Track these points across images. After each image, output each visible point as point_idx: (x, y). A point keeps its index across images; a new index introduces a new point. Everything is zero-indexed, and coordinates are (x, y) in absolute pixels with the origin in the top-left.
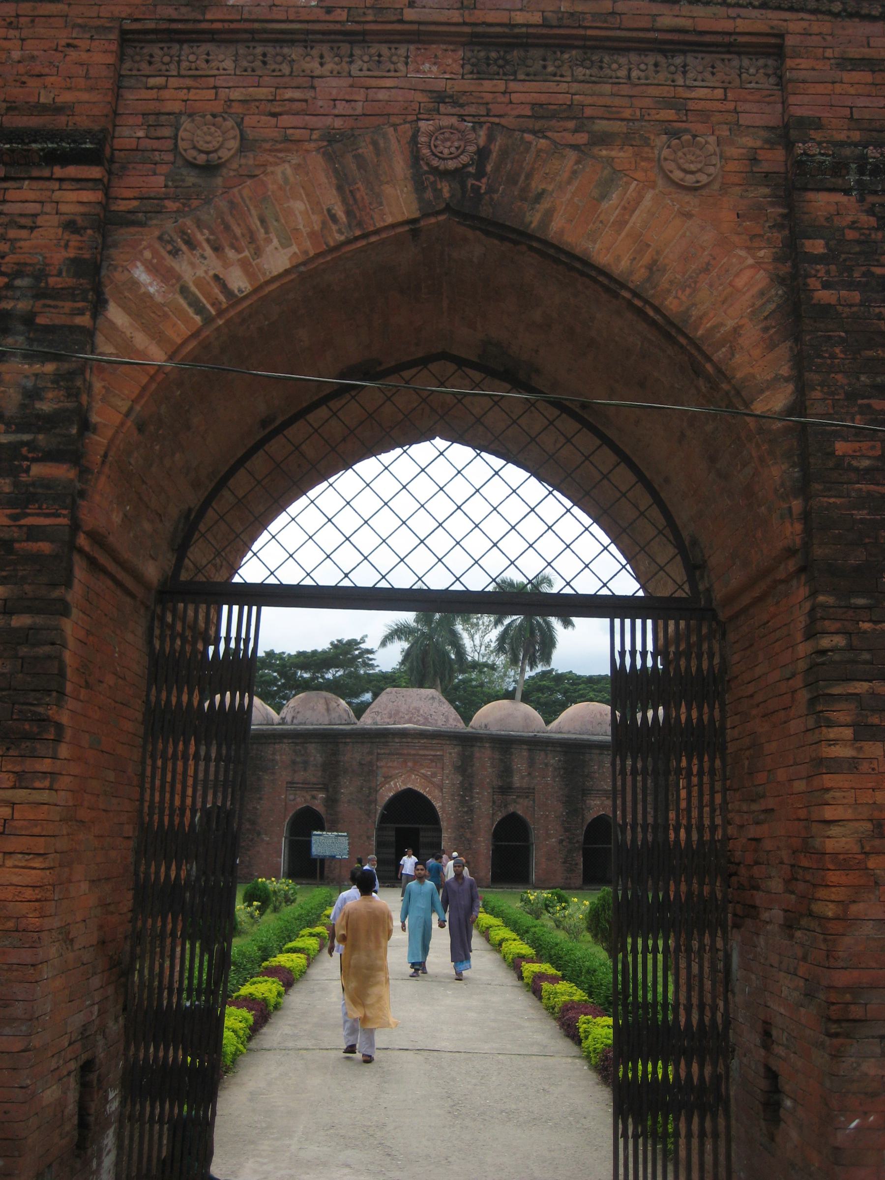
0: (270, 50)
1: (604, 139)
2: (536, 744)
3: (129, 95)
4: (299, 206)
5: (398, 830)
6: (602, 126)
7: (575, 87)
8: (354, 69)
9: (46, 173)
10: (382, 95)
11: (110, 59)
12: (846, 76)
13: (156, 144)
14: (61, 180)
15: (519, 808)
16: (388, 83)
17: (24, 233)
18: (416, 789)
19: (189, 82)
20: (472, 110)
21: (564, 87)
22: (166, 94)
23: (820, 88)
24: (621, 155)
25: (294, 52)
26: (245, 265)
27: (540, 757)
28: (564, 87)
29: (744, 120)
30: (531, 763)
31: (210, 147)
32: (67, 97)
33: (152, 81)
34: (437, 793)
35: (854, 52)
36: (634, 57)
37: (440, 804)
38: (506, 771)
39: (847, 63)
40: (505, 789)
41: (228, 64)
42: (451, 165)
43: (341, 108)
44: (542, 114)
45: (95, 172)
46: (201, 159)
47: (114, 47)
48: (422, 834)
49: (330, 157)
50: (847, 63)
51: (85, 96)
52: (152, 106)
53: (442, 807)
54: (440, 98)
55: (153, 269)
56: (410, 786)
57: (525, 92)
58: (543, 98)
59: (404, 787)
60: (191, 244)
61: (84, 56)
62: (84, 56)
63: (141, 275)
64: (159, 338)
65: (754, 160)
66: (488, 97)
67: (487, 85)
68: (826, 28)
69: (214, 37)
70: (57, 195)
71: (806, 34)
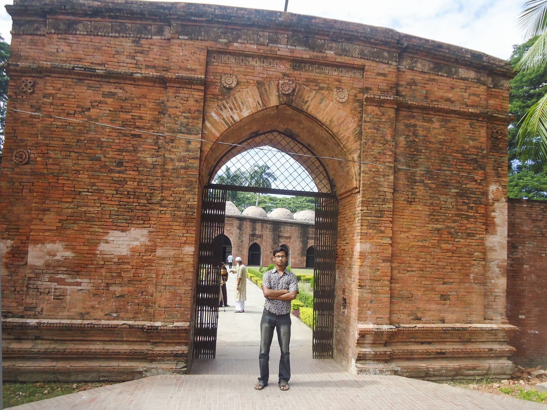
0: (244, 58)
1: (322, 88)
2: (264, 222)
4: (251, 100)
6: (321, 85)
7: (316, 74)
8: (264, 65)
9: (190, 87)
10: (271, 73)
11: (205, 58)
12: (379, 77)
13: (216, 81)
14: (194, 89)
15: (257, 241)
16: (272, 70)
17: (185, 102)
19: (224, 65)
20: (292, 78)
21: (313, 74)
22: (219, 67)
23: (372, 80)
24: (325, 92)
25: (250, 59)
27: (265, 225)
28: (313, 74)
29: (354, 86)
30: (262, 227)
31: (229, 83)
32: (194, 67)
33: (215, 64)
35: (381, 72)
36: (330, 68)
38: (254, 229)
39: (379, 74)
40: (253, 235)
41: (234, 61)
42: (287, 93)
43: (261, 75)
44: (308, 80)
45: (203, 88)
46: (228, 86)
47: (206, 54)
49: (258, 88)
50: (379, 74)
54: (285, 75)
55: (217, 113)
57: (305, 75)
58: (308, 77)
60: (225, 108)
61: (198, 56)
62: (198, 56)
63: (213, 114)
64: (218, 130)
65: (356, 96)
66: (296, 75)
67: (296, 72)
69: (229, 53)
71: (370, 66)
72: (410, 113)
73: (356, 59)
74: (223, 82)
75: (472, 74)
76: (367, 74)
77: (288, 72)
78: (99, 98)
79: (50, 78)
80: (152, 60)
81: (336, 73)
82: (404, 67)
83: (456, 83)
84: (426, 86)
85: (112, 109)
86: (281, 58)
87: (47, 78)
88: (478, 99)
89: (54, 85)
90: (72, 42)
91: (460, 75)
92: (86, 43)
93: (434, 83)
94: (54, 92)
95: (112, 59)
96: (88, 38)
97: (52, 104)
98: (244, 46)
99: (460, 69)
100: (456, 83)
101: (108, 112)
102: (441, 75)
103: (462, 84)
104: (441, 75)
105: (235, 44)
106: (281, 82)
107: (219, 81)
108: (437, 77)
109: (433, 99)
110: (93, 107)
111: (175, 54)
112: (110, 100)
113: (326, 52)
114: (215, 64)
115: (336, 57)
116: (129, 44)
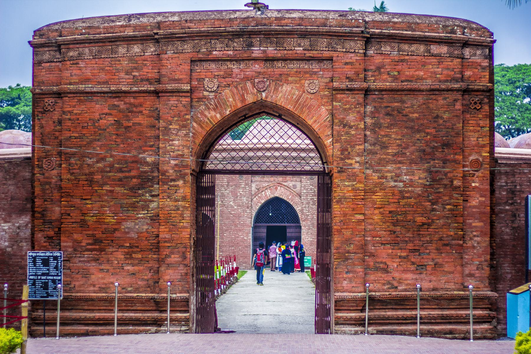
0: (223, 62)
3: (193, 74)
5: (268, 228)
7: (288, 70)
8: (241, 66)
10: (247, 73)
12: (346, 67)
16: (248, 70)
17: (175, 108)
18: (281, 197)
19: (206, 71)
20: (266, 76)
21: (286, 70)
23: (340, 70)
25: (228, 63)
26: (220, 113)
28: (286, 70)
32: (181, 77)
34: (297, 199)
35: (348, 61)
37: (300, 208)
41: (214, 66)
43: (238, 76)
45: (189, 94)
46: (210, 90)
48: (288, 230)
50: (346, 64)
51: (185, 77)
52: (199, 77)
53: (302, 211)
54: (259, 73)
56: (277, 195)
59: (272, 196)
61: (184, 67)
62: (184, 67)
66: (270, 73)
68: (342, 54)
70: (181, 99)
71: (338, 56)
72: (380, 96)
73: (324, 52)
74: (206, 87)
75: (444, 49)
76: (336, 65)
77: (262, 71)
78: (106, 111)
79: (67, 98)
80: (146, 74)
81: (306, 67)
82: (372, 52)
83: (427, 61)
84: (396, 67)
85: (116, 119)
86: (255, 60)
87: (65, 98)
88: (453, 73)
89: (70, 103)
90: (81, 66)
91: (432, 51)
92: (93, 65)
93: (405, 64)
94: (70, 109)
95: (114, 77)
96: (93, 62)
97: (70, 119)
98: (222, 53)
99: (432, 46)
100: (427, 61)
101: (113, 122)
102: (411, 55)
103: (434, 60)
104: (411, 55)
105: (214, 53)
106: (256, 80)
107: (202, 86)
108: (407, 57)
109: (403, 79)
110: (101, 119)
111: (164, 67)
112: (114, 112)
113: (296, 48)
114: (198, 71)
115: (305, 52)
116: (126, 62)
